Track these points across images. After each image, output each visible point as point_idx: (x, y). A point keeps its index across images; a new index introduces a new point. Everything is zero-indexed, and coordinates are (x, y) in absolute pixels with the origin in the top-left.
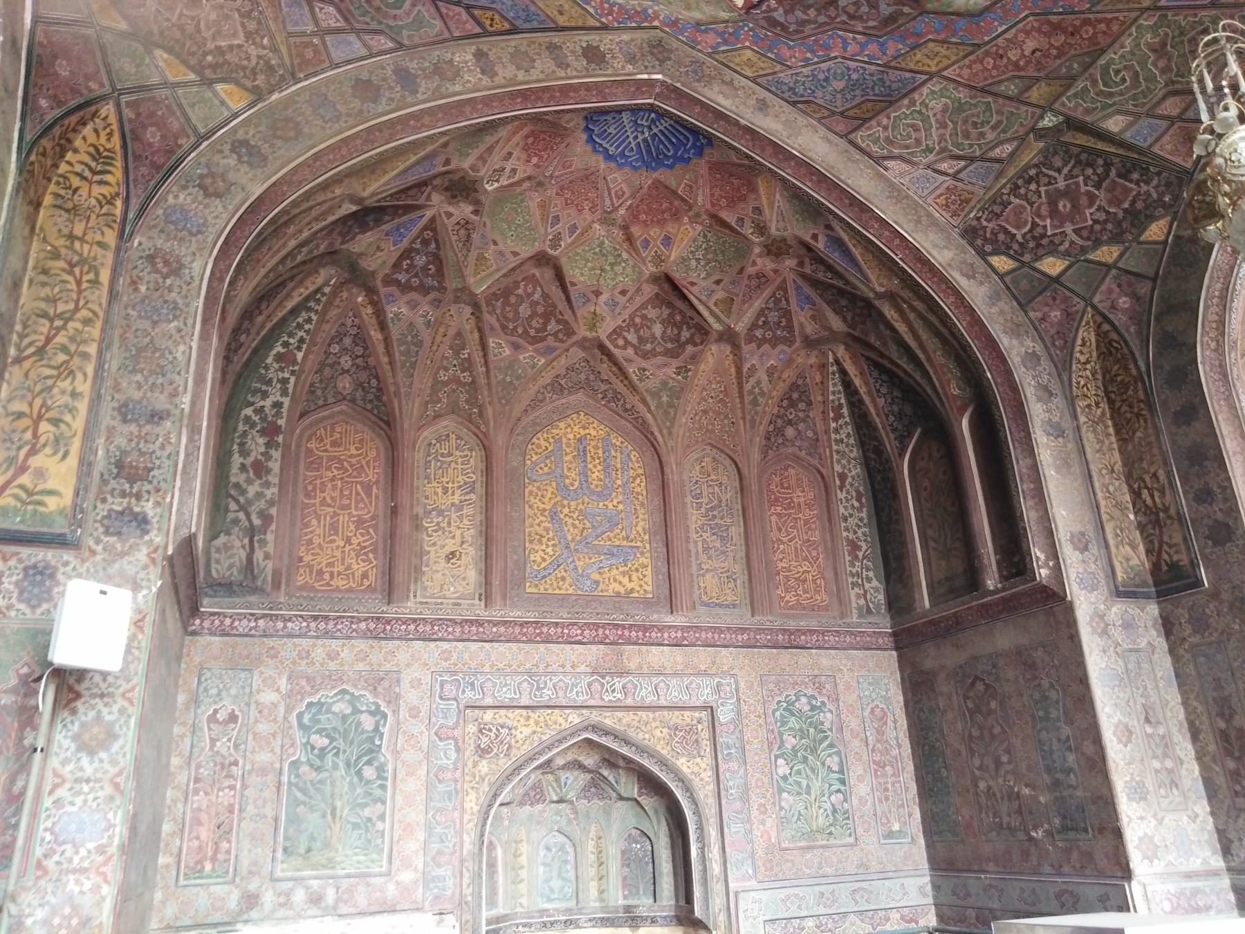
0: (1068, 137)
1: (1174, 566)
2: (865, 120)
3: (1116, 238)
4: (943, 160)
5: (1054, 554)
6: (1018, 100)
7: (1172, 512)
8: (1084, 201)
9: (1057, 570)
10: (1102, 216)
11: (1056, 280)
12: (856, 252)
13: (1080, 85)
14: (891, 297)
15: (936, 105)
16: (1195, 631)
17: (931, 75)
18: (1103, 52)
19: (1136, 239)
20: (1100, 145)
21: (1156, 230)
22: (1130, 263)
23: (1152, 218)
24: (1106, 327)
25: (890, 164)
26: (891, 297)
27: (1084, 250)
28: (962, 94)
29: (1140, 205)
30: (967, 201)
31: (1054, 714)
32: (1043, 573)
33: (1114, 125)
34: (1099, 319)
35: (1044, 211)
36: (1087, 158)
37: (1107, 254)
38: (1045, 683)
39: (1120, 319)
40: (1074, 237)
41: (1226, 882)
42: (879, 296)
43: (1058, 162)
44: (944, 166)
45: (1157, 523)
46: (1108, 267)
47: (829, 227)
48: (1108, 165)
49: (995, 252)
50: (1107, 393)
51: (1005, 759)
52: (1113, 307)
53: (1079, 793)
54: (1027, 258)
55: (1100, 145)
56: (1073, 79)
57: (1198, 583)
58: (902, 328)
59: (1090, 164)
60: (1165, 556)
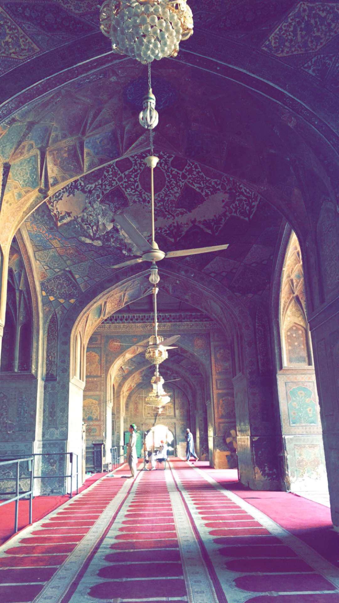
0: (68, 273)
1: (52, 375)
2: (40, 250)
3: (64, 299)
4: (46, 265)
5: (37, 368)
6: (65, 262)
7: (55, 363)
8: (63, 287)
9: (37, 371)
10: (64, 292)
11: (51, 302)
12: (22, 279)
13: (76, 265)
14: (21, 292)
15: (52, 254)
16: (52, 390)
17: (55, 248)
18: (82, 262)
19: (68, 301)
20: (72, 279)
21: (72, 301)
22: (65, 305)
23: (73, 298)
24: (55, 316)
25: (38, 261)
26: (21, 292)
27: (58, 298)
28: (57, 254)
29: (72, 294)
30: (45, 277)
31: (24, 404)
32: (33, 371)
33: (77, 276)
34: (54, 314)
35: (56, 286)
36: (69, 279)
37: (62, 301)
38: (24, 397)
39: (58, 316)
40: (58, 293)
41: (41, 443)
42: (18, 289)
43: (63, 277)
44: (45, 267)
45: (51, 364)
46: (62, 304)
47: (21, 271)
48: (71, 283)
49: (44, 291)
50: (48, 331)
51: (5, 414)
52: (58, 313)
53: (26, 423)
54: (48, 294)
55: (72, 279)
56: (75, 264)
57: (56, 380)
58: (18, 298)
59: (68, 281)
60: (50, 372)
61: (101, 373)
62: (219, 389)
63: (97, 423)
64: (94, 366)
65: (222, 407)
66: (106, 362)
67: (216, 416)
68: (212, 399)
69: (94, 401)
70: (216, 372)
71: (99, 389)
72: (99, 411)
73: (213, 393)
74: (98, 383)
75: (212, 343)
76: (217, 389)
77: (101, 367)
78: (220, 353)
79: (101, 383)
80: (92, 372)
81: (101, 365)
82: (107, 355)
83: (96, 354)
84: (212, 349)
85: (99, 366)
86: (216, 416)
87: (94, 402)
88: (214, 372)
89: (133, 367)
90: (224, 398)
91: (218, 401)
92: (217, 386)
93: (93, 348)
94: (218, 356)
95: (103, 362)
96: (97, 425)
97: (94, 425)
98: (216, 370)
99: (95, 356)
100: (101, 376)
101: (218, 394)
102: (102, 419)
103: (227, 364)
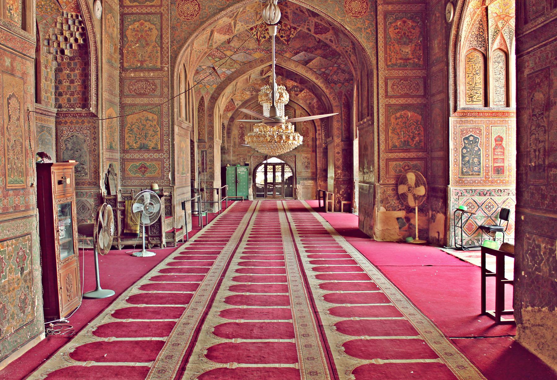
61: (161, 63)
62: (391, 97)
63: (156, 155)
64: (149, 49)
65: (394, 130)
66: (172, 42)
67: (382, 147)
68: (375, 115)
69: (150, 116)
70: (387, 65)
71: (158, 92)
72: (159, 133)
73: (378, 103)
74: (158, 82)
75: (380, 8)
76: (387, 96)
77: (161, 51)
78: (396, 28)
79: (162, 83)
80: (145, 61)
81: (162, 48)
82: (172, 28)
83: (153, 26)
84: (380, 18)
85: (159, 48)
86: (382, 147)
87: (150, 118)
88: (381, 64)
89: (233, 70)
90: (398, 115)
91: (387, 118)
92: (386, 92)
93: (147, 14)
94: (392, 32)
95: (165, 40)
96: (156, 160)
97: (152, 160)
98: (386, 60)
99: (150, 29)
100: (161, 69)
101: (388, 106)
102: (165, 148)
103: (407, 50)
